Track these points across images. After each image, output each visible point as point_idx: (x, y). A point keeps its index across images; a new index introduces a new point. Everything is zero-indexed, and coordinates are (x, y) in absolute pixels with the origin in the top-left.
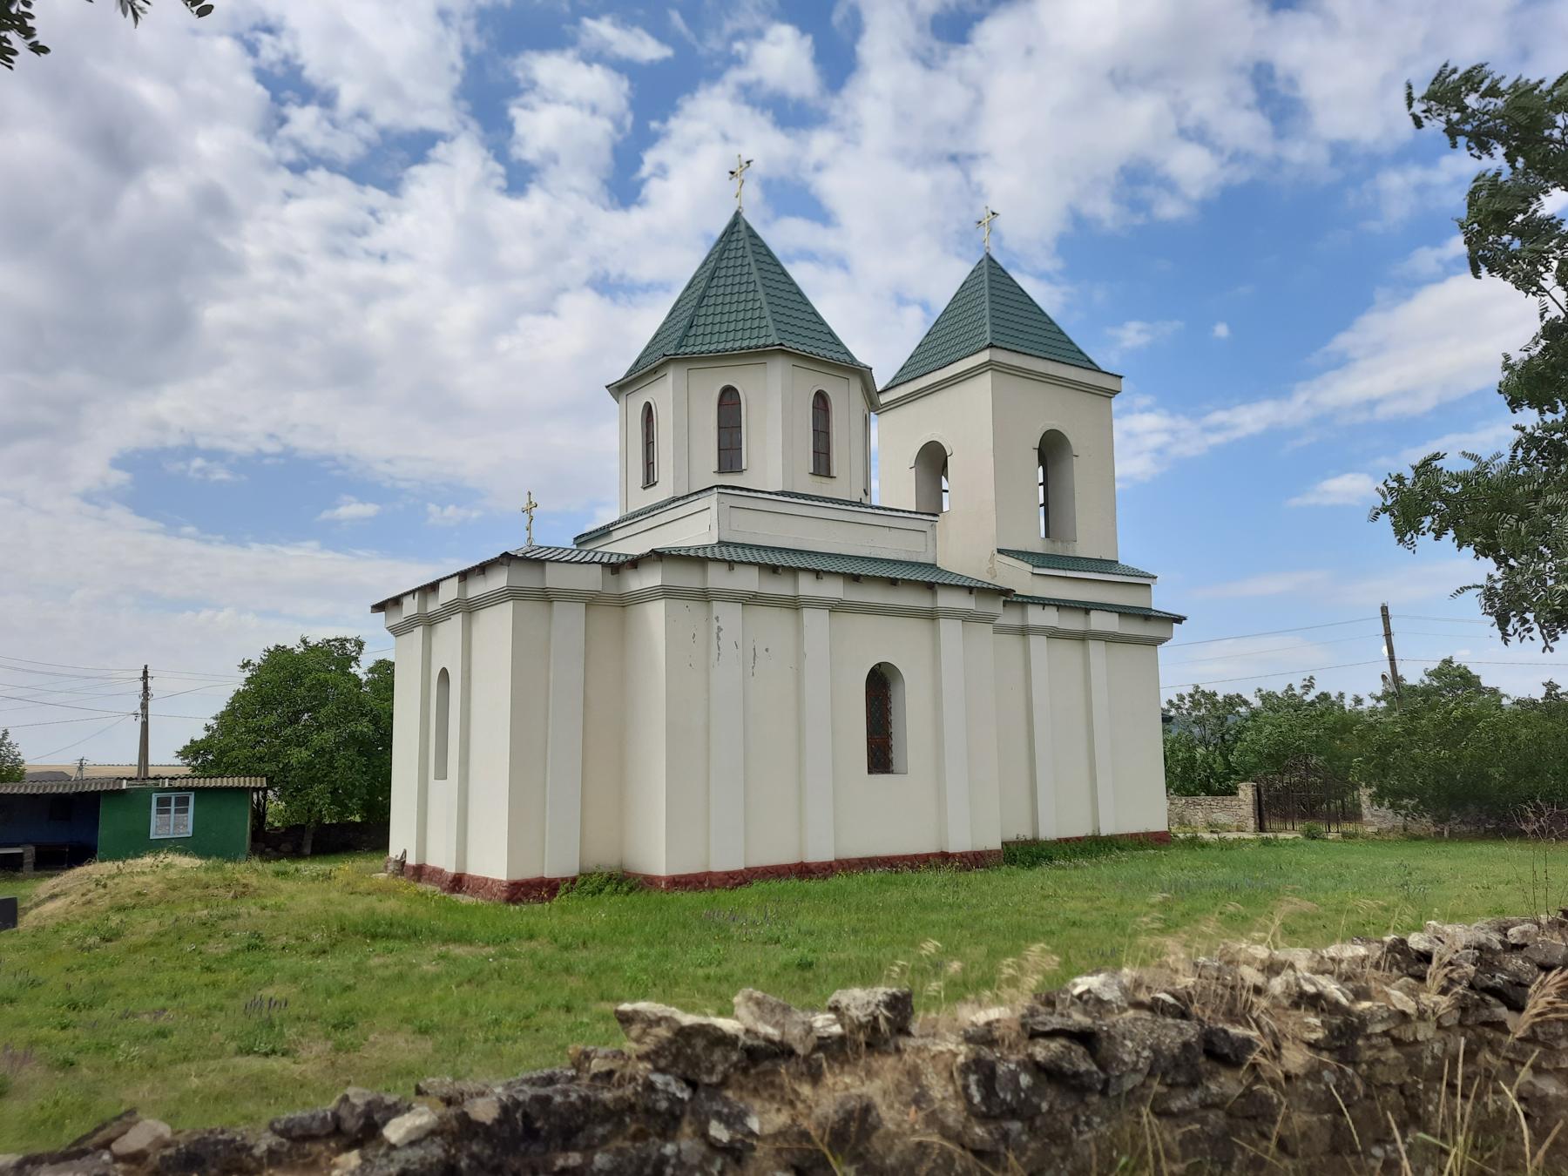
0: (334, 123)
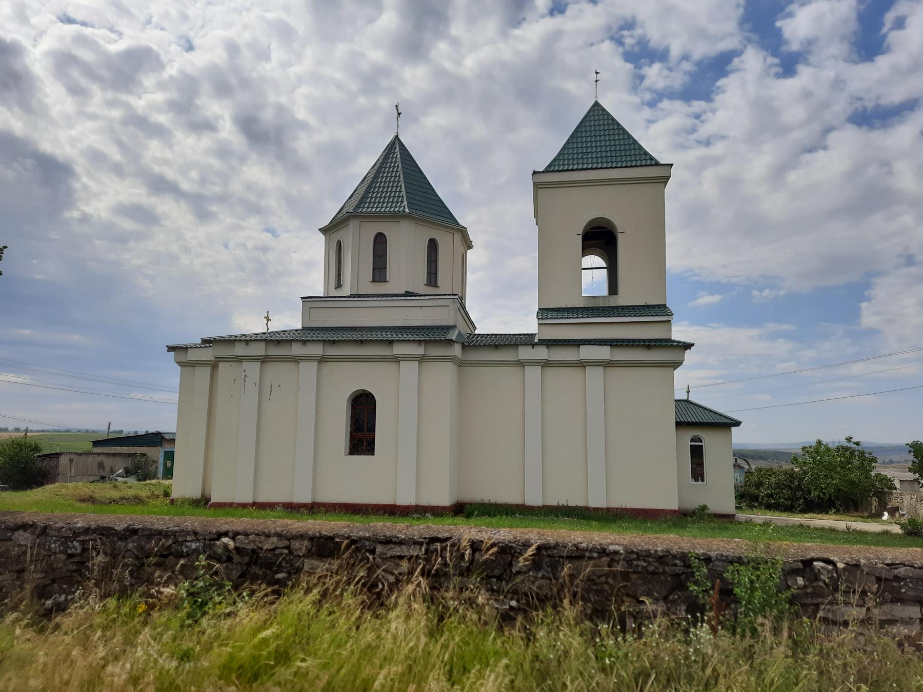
0: (670, 70)
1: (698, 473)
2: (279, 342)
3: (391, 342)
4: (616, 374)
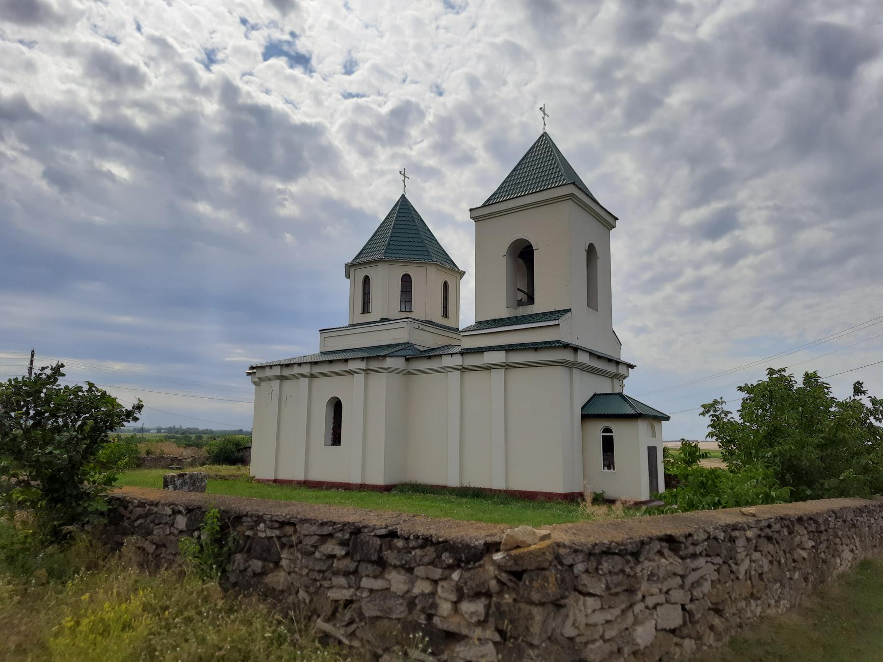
1: (609, 461)
2: (288, 365)
3: (346, 360)
4: (516, 375)
